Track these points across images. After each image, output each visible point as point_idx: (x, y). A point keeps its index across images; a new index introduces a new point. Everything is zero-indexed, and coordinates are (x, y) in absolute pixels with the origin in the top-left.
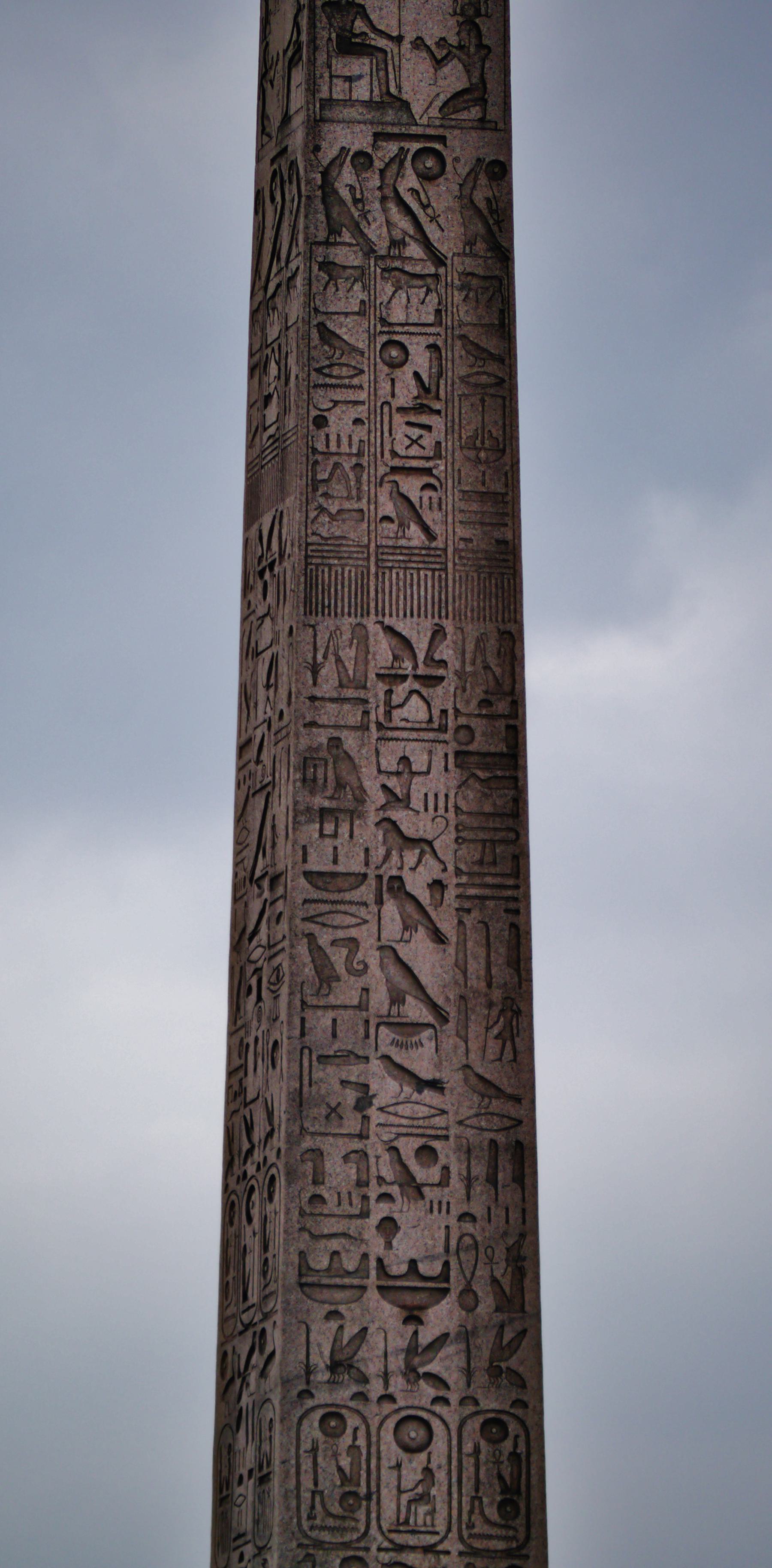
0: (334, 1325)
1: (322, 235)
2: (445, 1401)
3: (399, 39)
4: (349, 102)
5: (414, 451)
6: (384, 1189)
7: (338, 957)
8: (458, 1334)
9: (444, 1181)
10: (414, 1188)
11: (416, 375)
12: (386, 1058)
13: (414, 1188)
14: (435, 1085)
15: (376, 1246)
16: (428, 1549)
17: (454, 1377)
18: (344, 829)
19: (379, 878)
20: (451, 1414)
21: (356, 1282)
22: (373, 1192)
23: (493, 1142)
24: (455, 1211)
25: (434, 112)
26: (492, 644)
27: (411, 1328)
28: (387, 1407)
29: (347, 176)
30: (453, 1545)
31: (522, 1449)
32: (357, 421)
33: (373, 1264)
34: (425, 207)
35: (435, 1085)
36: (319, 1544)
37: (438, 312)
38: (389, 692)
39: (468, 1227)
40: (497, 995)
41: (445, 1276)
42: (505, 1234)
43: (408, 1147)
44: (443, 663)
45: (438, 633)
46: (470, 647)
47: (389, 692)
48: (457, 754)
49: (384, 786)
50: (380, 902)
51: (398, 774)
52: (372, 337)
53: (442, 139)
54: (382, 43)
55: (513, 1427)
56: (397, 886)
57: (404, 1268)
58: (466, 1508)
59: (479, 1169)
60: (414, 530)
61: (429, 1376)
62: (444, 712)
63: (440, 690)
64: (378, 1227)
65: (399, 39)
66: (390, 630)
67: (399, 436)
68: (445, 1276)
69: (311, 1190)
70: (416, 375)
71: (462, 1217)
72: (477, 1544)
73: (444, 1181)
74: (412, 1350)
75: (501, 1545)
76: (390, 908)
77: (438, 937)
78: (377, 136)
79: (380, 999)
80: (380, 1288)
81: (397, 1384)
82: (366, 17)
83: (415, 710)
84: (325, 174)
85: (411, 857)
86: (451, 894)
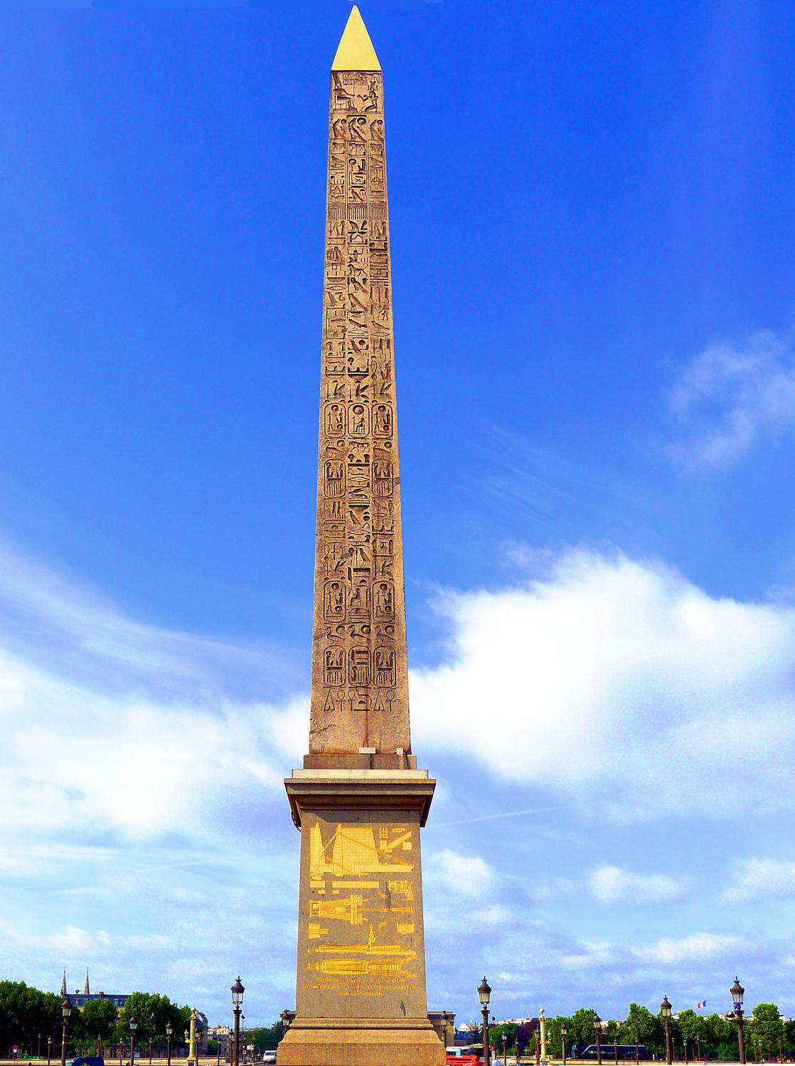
0: (335, 384)
1: (333, 137)
2: (368, 402)
3: (354, 95)
4: (341, 109)
5: (358, 182)
6: (350, 351)
7: (336, 297)
8: (371, 386)
9: (367, 348)
10: (357, 350)
11: (359, 166)
12: (350, 320)
13: (357, 350)
14: (364, 326)
15: (348, 365)
16: (362, 438)
17: (371, 398)
18: (339, 267)
19: (348, 278)
20: (369, 405)
21: (342, 373)
22: (347, 351)
23: (381, 339)
24: (370, 356)
25: (363, 110)
26: (380, 224)
27: (358, 384)
28: (351, 403)
29: (340, 124)
30: (370, 437)
31: (390, 413)
32: (343, 177)
33: (346, 369)
34: (361, 130)
35: (364, 326)
36: (331, 438)
37: (364, 153)
38: (351, 236)
39: (374, 359)
40: (382, 304)
41: (367, 371)
42: (385, 361)
43: (357, 341)
44: (366, 229)
45: (365, 223)
46: (373, 225)
47: (351, 236)
48: (370, 249)
49: (350, 258)
50: (348, 284)
51: (354, 254)
52: (346, 159)
53: (365, 116)
54: (349, 96)
55: (387, 408)
56: (354, 281)
57: (356, 370)
58: (374, 428)
59: (377, 345)
60: (359, 201)
61: (362, 396)
62: (367, 240)
63: (365, 235)
64: (348, 360)
65: (354, 95)
66: (351, 222)
67: (354, 179)
68: (367, 371)
69: (330, 352)
70: (359, 166)
71: (372, 357)
72: (377, 437)
73: (367, 348)
74: (357, 390)
75: (385, 437)
76: (351, 285)
77: (365, 291)
78: (348, 116)
79: (348, 307)
80: (349, 375)
81: (354, 398)
82: (345, 92)
83: (359, 239)
84: (334, 125)
85: (357, 273)
86: (368, 281)
